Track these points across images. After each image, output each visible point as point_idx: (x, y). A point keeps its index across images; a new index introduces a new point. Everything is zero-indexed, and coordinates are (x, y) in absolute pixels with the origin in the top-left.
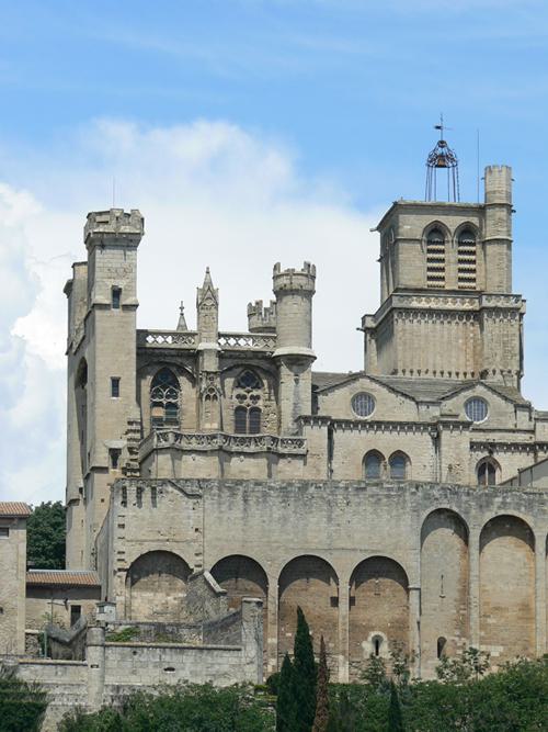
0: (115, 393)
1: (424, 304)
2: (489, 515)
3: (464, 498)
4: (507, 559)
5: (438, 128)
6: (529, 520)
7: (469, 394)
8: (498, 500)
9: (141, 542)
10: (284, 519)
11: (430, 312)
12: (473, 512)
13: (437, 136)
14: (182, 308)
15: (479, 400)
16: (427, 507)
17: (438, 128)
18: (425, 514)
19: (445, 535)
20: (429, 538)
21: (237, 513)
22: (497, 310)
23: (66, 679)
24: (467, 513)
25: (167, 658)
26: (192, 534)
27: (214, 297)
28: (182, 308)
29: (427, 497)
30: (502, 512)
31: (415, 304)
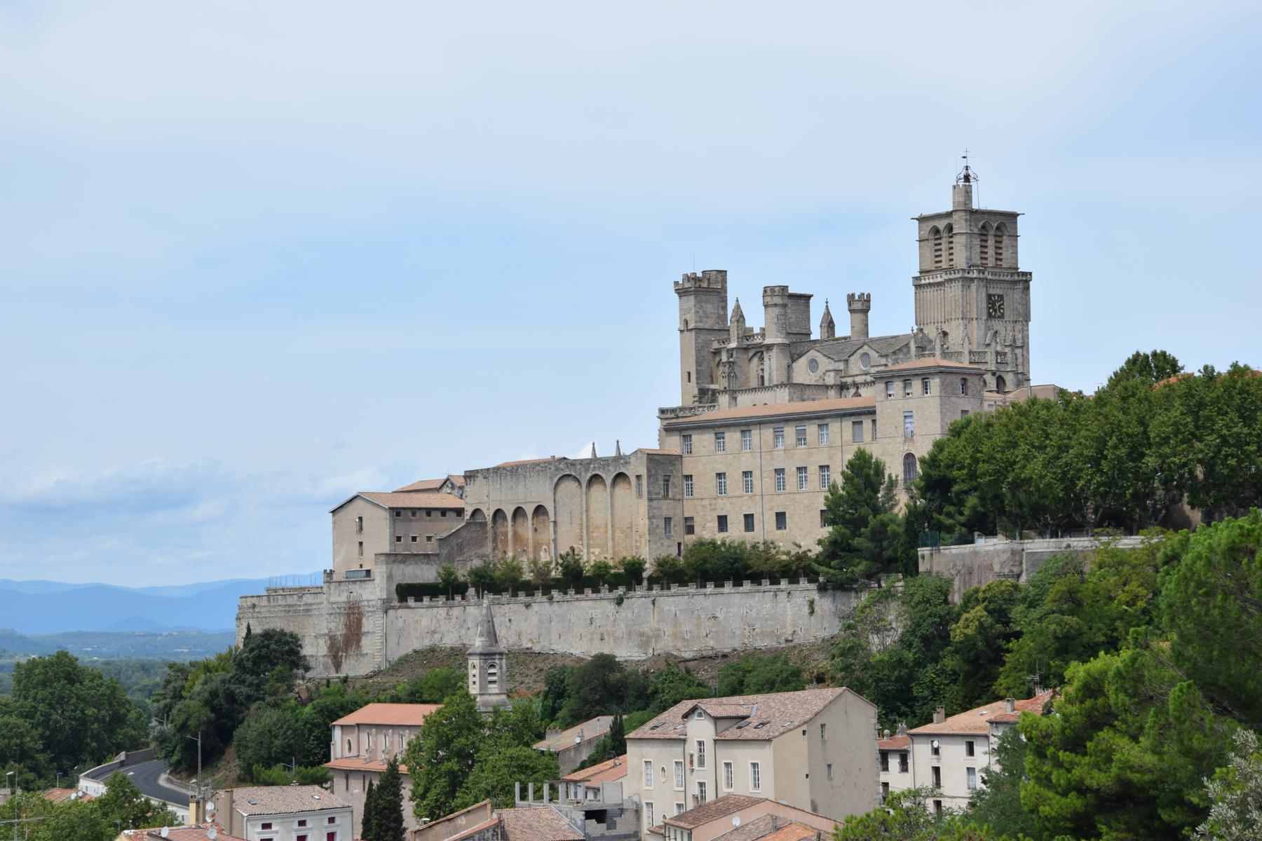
0: (689, 381)
1: (927, 281)
2: (589, 475)
3: (578, 467)
4: (600, 499)
5: (964, 157)
6: (603, 475)
7: (860, 351)
8: (592, 466)
9: (472, 504)
10: (512, 487)
11: (930, 285)
12: (583, 474)
13: (964, 163)
14: (827, 303)
15: (866, 354)
16: (557, 475)
17: (964, 157)
18: (556, 480)
19: (573, 485)
20: (559, 494)
21: (498, 486)
22: (950, 280)
23: (317, 601)
24: (580, 475)
25: (350, 587)
26: (486, 499)
27: (742, 316)
28: (827, 303)
29: (557, 469)
30: (594, 473)
31: (923, 282)
